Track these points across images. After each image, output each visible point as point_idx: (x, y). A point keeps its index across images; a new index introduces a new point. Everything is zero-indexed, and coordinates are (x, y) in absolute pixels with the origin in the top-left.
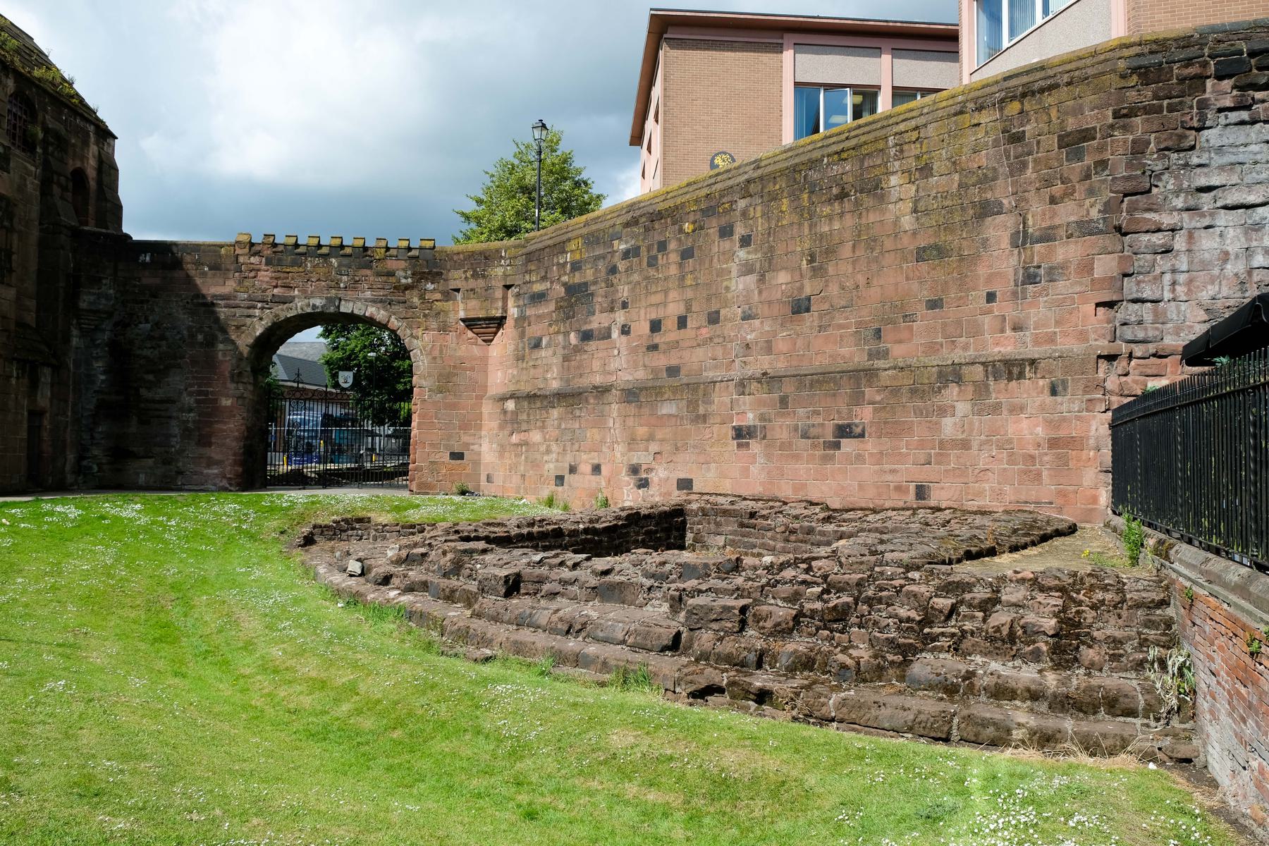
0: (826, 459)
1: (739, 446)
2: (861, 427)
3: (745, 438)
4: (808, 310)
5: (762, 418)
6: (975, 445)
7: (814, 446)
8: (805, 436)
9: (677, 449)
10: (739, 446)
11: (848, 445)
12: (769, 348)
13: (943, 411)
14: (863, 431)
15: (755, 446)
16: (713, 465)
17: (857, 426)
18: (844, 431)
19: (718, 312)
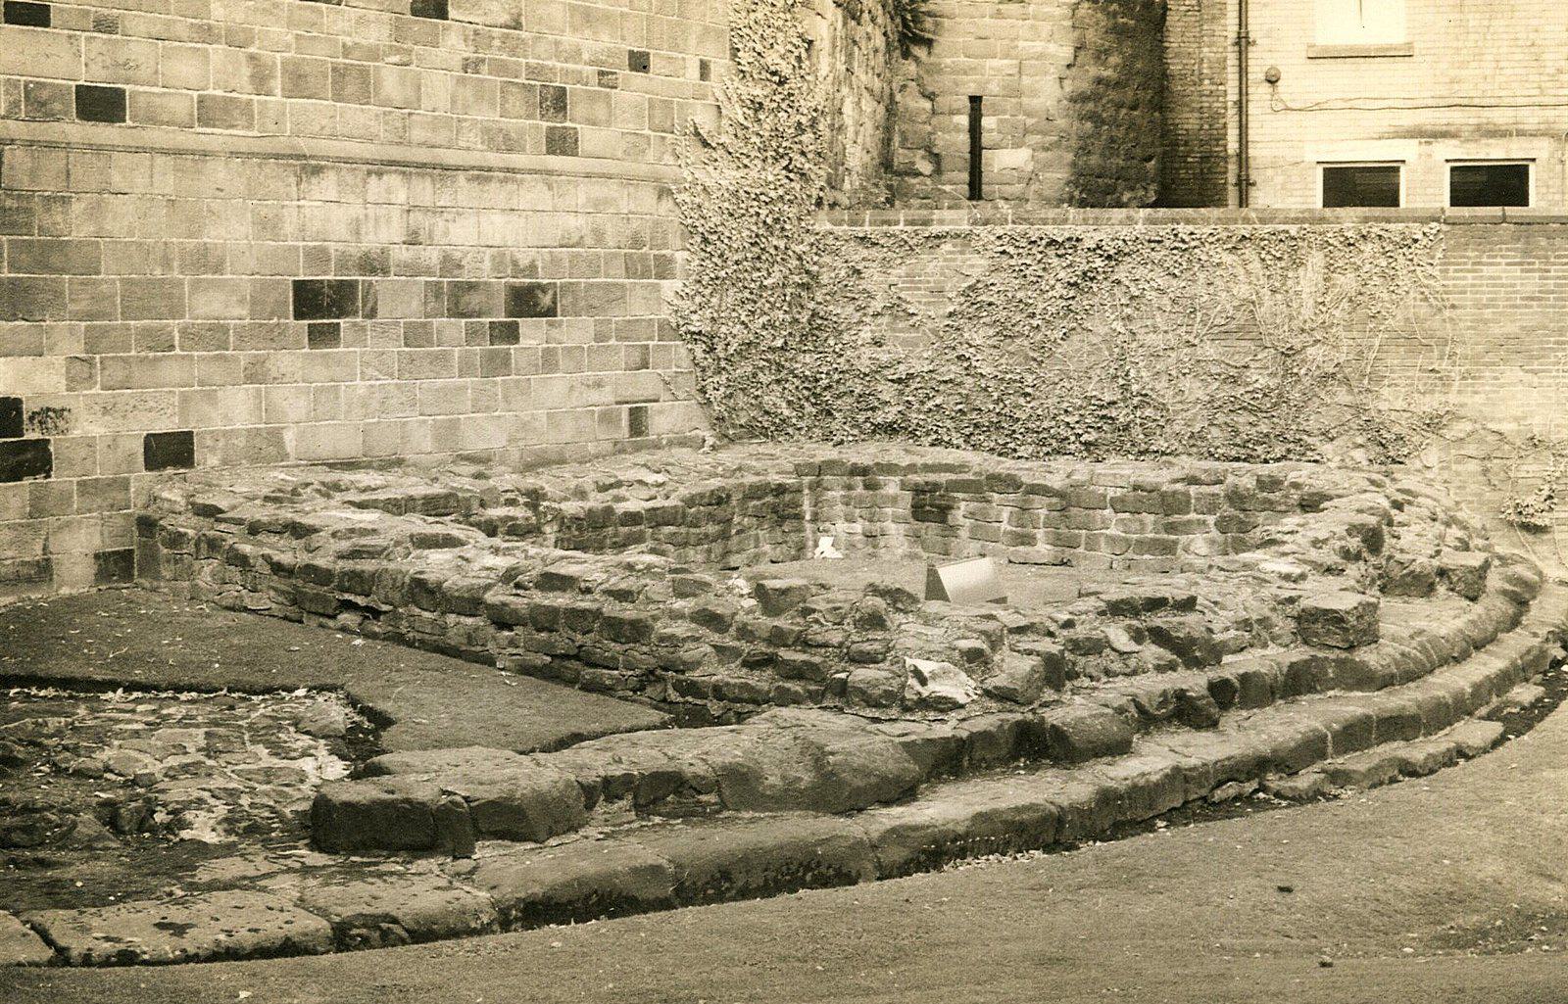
0: (497, 365)
2: (551, 292)
7: (472, 334)
11: (533, 333)
14: (554, 303)
17: (543, 289)
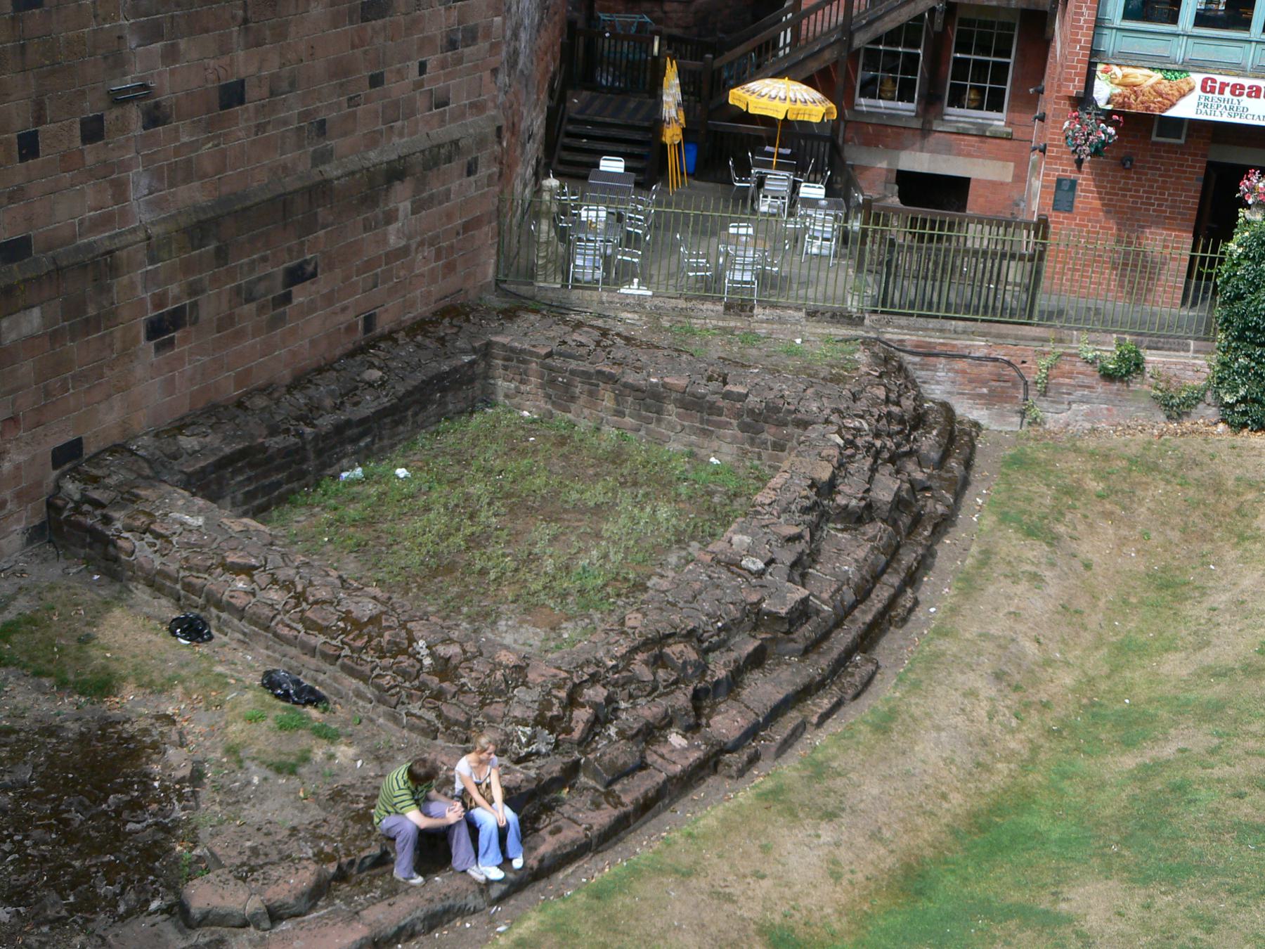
1: (159, 348)
3: (168, 331)
4: (241, 101)
5: (194, 290)
6: (414, 246)
7: (261, 310)
8: (250, 299)
9: (48, 394)
10: (159, 348)
11: (301, 294)
12: (186, 172)
13: (390, 218)
14: (316, 268)
15: (184, 341)
16: (117, 397)
18: (297, 275)
19: (100, 119)
